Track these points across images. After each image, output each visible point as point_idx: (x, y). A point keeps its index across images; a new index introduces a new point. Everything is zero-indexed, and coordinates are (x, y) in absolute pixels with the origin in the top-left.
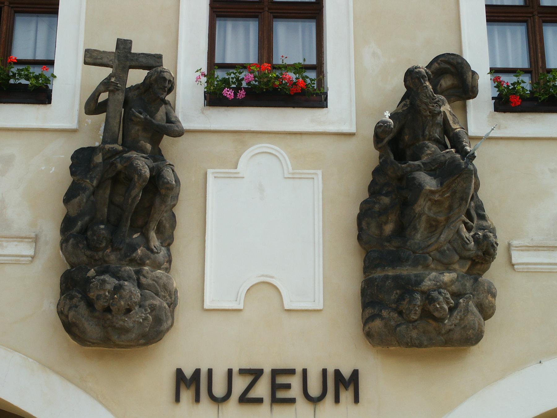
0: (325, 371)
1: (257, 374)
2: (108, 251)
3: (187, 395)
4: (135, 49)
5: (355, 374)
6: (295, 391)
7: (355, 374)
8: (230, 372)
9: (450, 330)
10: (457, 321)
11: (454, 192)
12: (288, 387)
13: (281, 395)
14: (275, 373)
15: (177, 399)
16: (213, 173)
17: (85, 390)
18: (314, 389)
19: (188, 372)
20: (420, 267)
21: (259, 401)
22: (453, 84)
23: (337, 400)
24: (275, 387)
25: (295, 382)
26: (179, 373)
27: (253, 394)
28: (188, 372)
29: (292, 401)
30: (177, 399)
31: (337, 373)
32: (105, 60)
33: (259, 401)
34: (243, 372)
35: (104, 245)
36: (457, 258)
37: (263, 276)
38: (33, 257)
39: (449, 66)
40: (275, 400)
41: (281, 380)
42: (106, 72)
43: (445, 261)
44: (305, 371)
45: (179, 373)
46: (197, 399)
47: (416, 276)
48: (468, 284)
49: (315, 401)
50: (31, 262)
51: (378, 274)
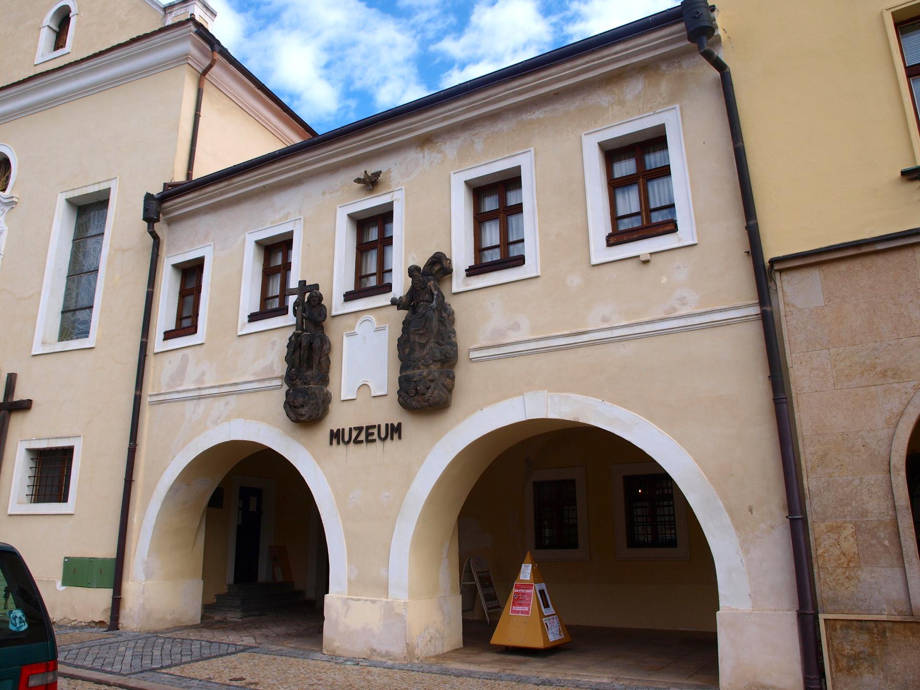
0: (387, 425)
2: (297, 380)
3: (335, 441)
5: (400, 424)
6: (375, 437)
7: (400, 424)
8: (350, 429)
9: (428, 399)
10: (430, 394)
11: (427, 329)
12: (373, 434)
13: (370, 438)
14: (368, 428)
15: (331, 443)
16: (346, 334)
18: (383, 435)
20: (416, 369)
21: (361, 442)
22: (440, 268)
24: (368, 435)
25: (375, 431)
26: (332, 431)
27: (359, 439)
29: (374, 441)
30: (331, 443)
31: (392, 425)
32: (294, 292)
33: (361, 442)
34: (356, 428)
36: (431, 362)
38: (282, 385)
40: (369, 441)
41: (370, 431)
43: (426, 364)
44: (379, 426)
45: (332, 431)
46: (338, 443)
47: (413, 374)
48: (436, 375)
50: (281, 387)
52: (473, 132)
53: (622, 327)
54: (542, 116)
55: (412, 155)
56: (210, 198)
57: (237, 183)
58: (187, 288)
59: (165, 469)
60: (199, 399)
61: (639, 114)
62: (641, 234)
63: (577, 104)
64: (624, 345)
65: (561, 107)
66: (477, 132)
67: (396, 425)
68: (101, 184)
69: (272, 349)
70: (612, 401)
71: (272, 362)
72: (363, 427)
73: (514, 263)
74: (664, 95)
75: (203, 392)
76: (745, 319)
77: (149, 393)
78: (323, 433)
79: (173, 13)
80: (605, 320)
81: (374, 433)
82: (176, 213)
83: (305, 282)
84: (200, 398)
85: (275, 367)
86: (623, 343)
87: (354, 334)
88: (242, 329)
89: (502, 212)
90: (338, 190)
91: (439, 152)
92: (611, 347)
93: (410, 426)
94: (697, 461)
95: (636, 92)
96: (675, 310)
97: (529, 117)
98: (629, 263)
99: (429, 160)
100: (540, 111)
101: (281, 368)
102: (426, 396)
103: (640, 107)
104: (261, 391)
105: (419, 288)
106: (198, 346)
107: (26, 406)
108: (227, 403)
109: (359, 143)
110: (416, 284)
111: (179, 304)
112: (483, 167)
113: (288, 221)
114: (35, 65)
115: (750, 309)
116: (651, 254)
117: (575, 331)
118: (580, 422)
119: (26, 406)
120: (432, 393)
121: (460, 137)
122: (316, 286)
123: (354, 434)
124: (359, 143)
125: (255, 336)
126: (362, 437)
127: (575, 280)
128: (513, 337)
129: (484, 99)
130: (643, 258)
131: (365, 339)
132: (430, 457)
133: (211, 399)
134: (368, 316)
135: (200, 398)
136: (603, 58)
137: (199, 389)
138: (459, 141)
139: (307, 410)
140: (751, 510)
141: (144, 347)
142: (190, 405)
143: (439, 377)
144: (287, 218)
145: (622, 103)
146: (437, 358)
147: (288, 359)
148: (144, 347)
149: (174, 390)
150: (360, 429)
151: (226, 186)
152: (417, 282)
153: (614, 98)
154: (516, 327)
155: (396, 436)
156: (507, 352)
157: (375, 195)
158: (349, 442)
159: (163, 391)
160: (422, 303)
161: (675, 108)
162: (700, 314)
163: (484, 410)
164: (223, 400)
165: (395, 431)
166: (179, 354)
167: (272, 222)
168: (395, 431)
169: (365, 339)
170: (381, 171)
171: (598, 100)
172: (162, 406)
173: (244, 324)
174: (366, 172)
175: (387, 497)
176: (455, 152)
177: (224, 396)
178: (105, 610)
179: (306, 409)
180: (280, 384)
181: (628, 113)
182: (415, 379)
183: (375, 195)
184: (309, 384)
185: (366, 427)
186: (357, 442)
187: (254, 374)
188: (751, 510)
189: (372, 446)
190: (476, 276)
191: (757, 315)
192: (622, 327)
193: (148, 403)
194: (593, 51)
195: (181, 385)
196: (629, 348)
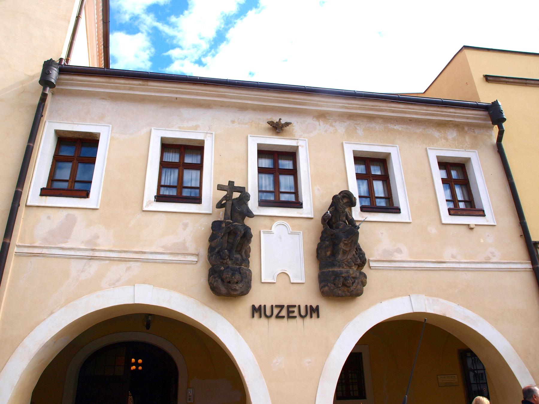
0: (306, 306)
1: (282, 307)
2: (228, 260)
3: (256, 315)
4: (235, 185)
5: (317, 307)
6: (296, 314)
7: (317, 307)
8: (272, 306)
9: (352, 291)
10: (355, 288)
11: (352, 241)
12: (293, 312)
13: (291, 315)
14: (289, 307)
15: (253, 316)
16: (263, 231)
17: (219, 313)
18: (303, 313)
19: (257, 306)
20: (341, 268)
21: (283, 317)
23: (311, 317)
24: (289, 312)
25: (296, 310)
26: (253, 307)
27: (281, 315)
28: (257, 306)
29: (295, 317)
30: (253, 316)
31: (311, 306)
32: (225, 189)
33: (283, 317)
35: (227, 258)
36: (354, 264)
37: (282, 270)
38: (197, 262)
39: (346, 195)
40: (289, 317)
41: (291, 309)
42: (225, 193)
43: (350, 266)
44: (299, 306)
45: (253, 307)
46: (260, 317)
48: (358, 274)
50: (196, 263)
51: (325, 270)
52: (355, 122)
53: (465, 263)
54: (400, 129)
55: (310, 120)
56: (117, 88)
57: (152, 86)
58: (61, 154)
59: (38, 324)
62: (467, 213)
63: (421, 130)
64: (465, 273)
65: (412, 129)
66: (358, 123)
67: (314, 306)
69: (184, 229)
70: (463, 305)
71: (184, 240)
72: (284, 306)
73: (378, 210)
75: (97, 254)
76: (525, 270)
77: (17, 244)
80: (453, 257)
81: (294, 311)
82: (69, 88)
83: (233, 182)
84: (92, 258)
85: (188, 244)
86: (465, 272)
87: (271, 233)
88: (147, 205)
89: (181, 165)
90: (246, 124)
91: (331, 125)
92: (459, 273)
93: (326, 308)
94: (511, 345)
95: (453, 136)
96: (490, 258)
97: (392, 127)
98: (462, 226)
99: (324, 128)
100: (399, 126)
102: (352, 288)
103: (457, 145)
104: (172, 263)
105: (341, 212)
106: (90, 210)
108: (128, 269)
109: (237, 95)
110: (341, 208)
111: (52, 166)
112: (365, 146)
113: (196, 131)
115: (527, 265)
116: (476, 225)
118: (447, 316)
120: (356, 287)
121: (346, 122)
123: (276, 311)
124: (237, 95)
125: (163, 215)
126: (284, 313)
127: (433, 230)
128: (398, 257)
129: (372, 106)
130: (472, 226)
131: (280, 238)
132: (344, 333)
133: (107, 262)
134: (287, 224)
135: (92, 258)
136: (443, 112)
137: (93, 250)
138: (346, 124)
139: (241, 286)
141: (17, 197)
143: (360, 276)
145: (446, 139)
146: (358, 263)
148: (17, 197)
149: (56, 246)
151: (140, 85)
152: (341, 207)
153: (441, 135)
154: (399, 251)
155: (314, 315)
156: (397, 266)
157: (282, 138)
159: (36, 244)
160: (341, 222)
162: (411, 262)
163: (383, 303)
164: (123, 266)
166: (65, 212)
169: (280, 238)
170: (291, 123)
171: (433, 133)
172: (34, 259)
173: (150, 203)
174: (280, 119)
175: (309, 363)
176: (344, 130)
177: (126, 261)
179: (240, 285)
180: (196, 260)
181: (450, 146)
182: (343, 275)
183: (282, 138)
184: (242, 266)
185: (288, 306)
187: (163, 247)
189: (292, 322)
190: (368, 213)
191: (530, 268)
192: (465, 263)
193: (14, 253)
194: (438, 106)
196: (469, 276)
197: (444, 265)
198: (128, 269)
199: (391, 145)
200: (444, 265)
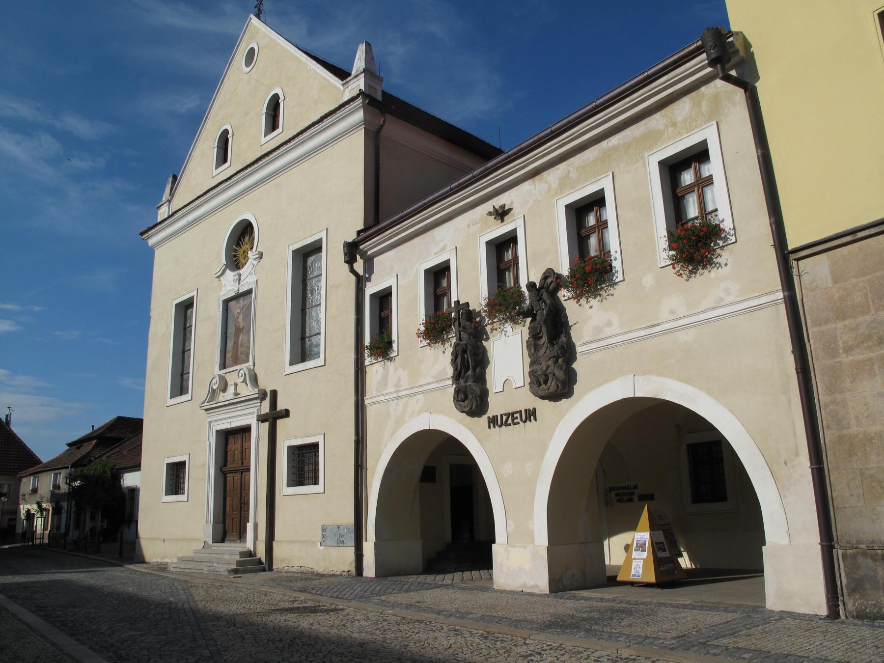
0: (526, 410)
5: (534, 409)
6: (519, 420)
8: (502, 416)
13: (516, 421)
14: (513, 413)
25: (518, 415)
29: (518, 423)
30: (489, 427)
41: (515, 415)
44: (521, 411)
49: (525, 422)
60: (399, 399)
61: (687, 133)
68: (316, 235)
74: (705, 113)
76: (774, 303)
78: (484, 419)
79: (350, 87)
80: (672, 312)
100: (615, 139)
101: (450, 371)
103: (688, 126)
107: (286, 414)
108: (417, 401)
114: (261, 146)
117: (650, 324)
119: (286, 414)
122: (467, 304)
123: (504, 418)
126: (510, 421)
128: (608, 331)
140: (786, 464)
142: (393, 404)
144: (445, 249)
147: (454, 362)
150: (508, 415)
154: (609, 324)
158: (500, 426)
159: (374, 395)
161: (713, 124)
165: (531, 414)
167: (435, 254)
168: (531, 414)
170: (505, 205)
174: (494, 206)
178: (351, 563)
186: (507, 425)
188: (786, 464)
195: (385, 389)
197: (657, 329)
198: (417, 401)
199: (603, 176)
200: (657, 329)
